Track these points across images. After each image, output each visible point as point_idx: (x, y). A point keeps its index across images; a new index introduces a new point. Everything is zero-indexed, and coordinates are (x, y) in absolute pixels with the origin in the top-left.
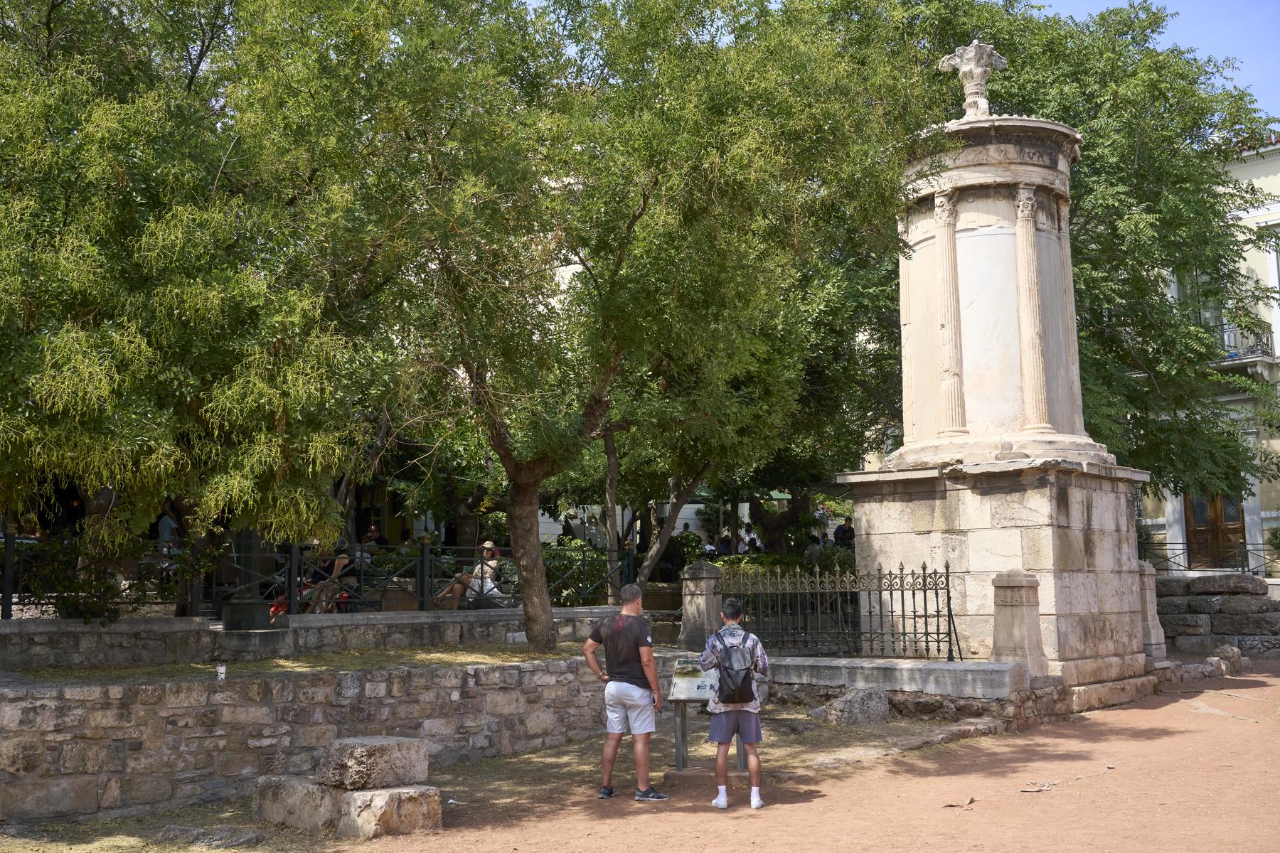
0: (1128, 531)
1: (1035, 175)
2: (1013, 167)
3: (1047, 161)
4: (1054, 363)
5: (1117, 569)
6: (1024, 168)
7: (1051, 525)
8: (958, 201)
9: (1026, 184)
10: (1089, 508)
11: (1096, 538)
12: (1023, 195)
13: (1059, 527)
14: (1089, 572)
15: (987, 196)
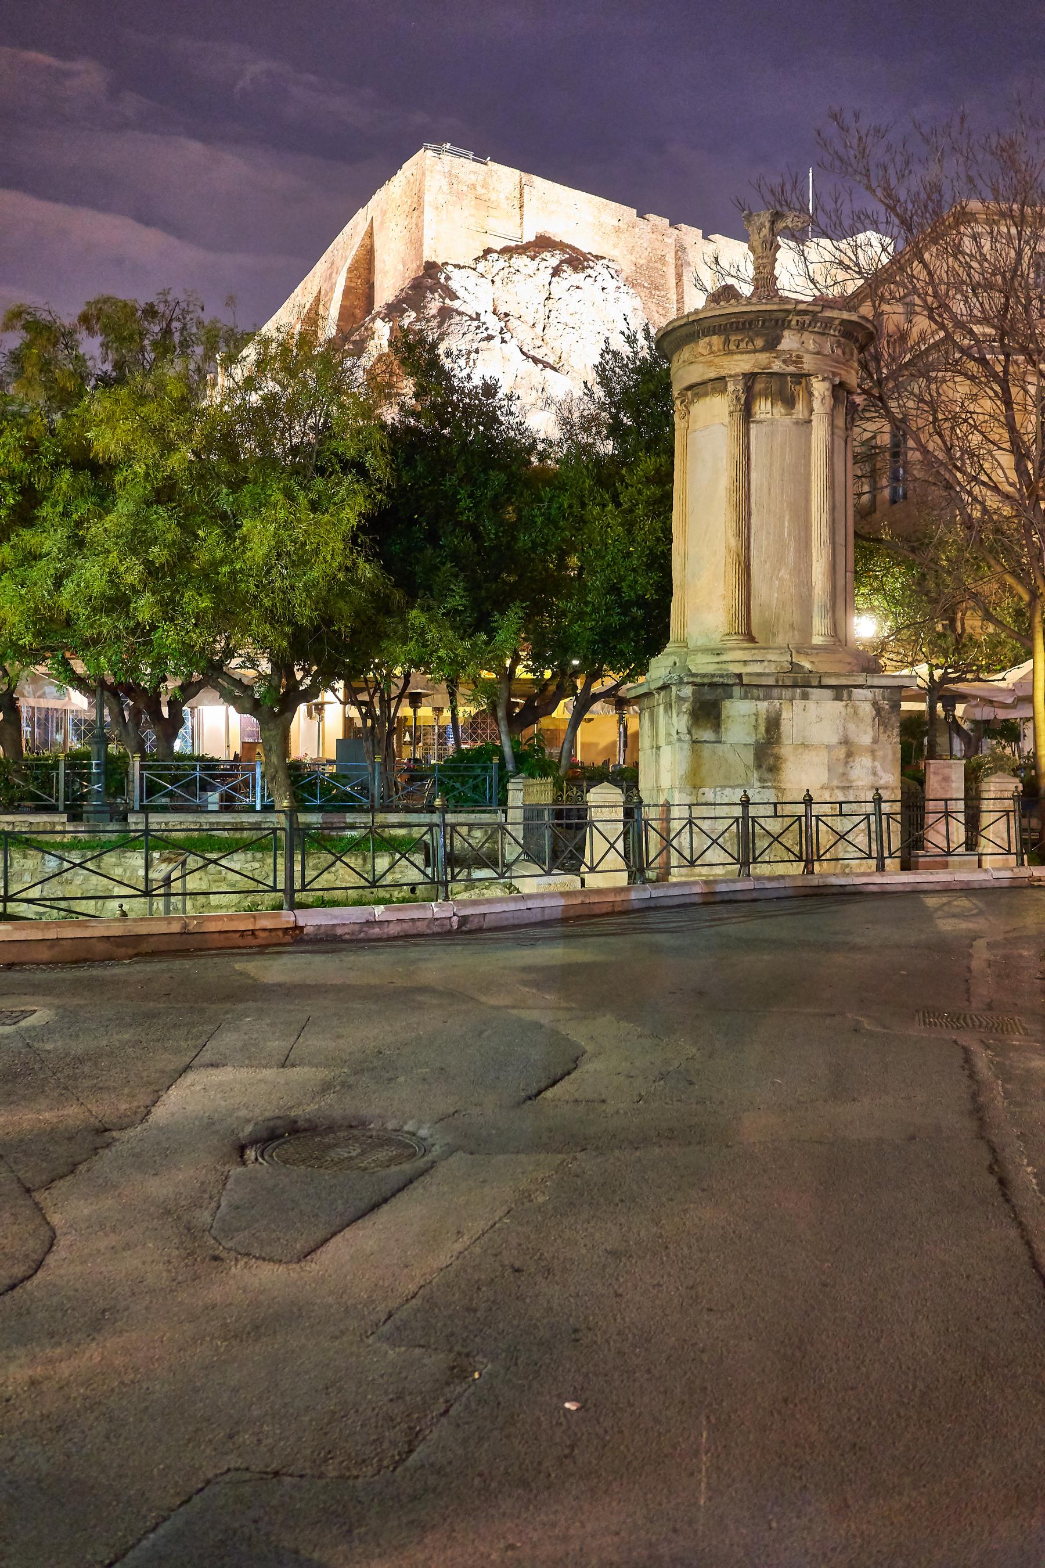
0: (875, 741)
1: (743, 364)
2: (717, 360)
3: (759, 343)
4: (767, 566)
5: (835, 783)
6: (729, 358)
7: (679, 740)
8: (692, 402)
9: (731, 376)
10: (773, 724)
11: (786, 750)
12: (731, 387)
13: (694, 742)
14: (763, 787)
15: (706, 395)
